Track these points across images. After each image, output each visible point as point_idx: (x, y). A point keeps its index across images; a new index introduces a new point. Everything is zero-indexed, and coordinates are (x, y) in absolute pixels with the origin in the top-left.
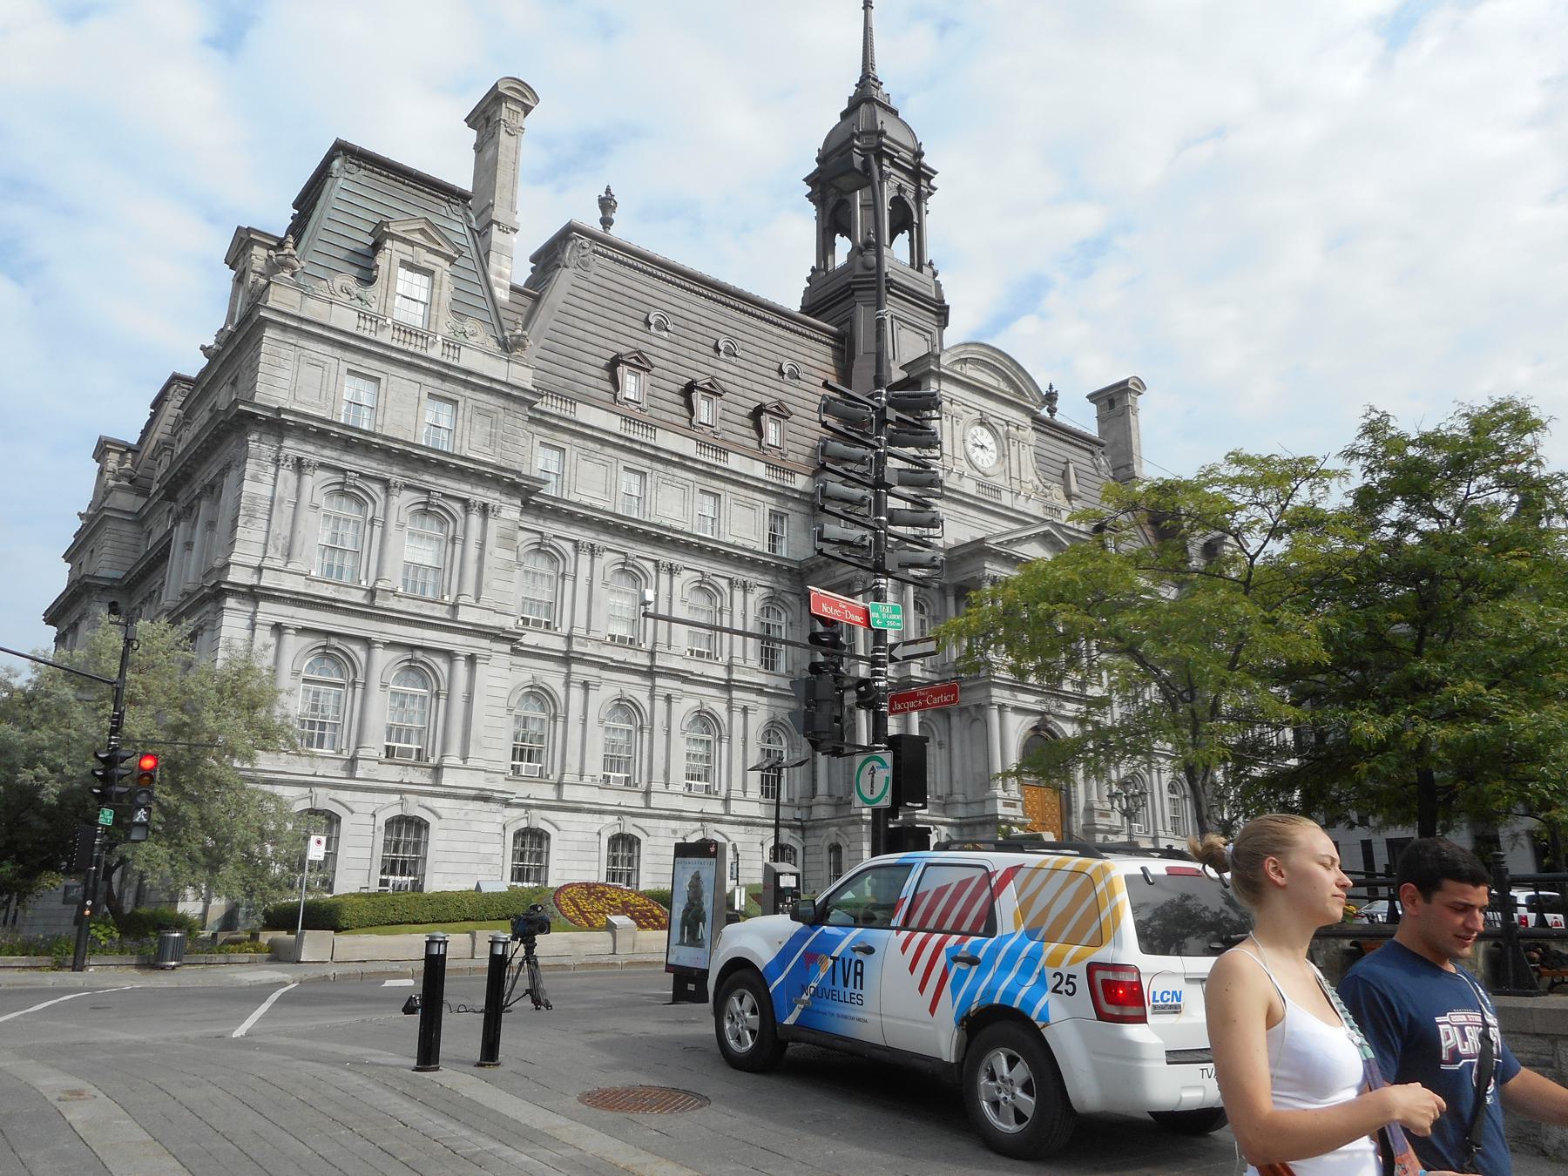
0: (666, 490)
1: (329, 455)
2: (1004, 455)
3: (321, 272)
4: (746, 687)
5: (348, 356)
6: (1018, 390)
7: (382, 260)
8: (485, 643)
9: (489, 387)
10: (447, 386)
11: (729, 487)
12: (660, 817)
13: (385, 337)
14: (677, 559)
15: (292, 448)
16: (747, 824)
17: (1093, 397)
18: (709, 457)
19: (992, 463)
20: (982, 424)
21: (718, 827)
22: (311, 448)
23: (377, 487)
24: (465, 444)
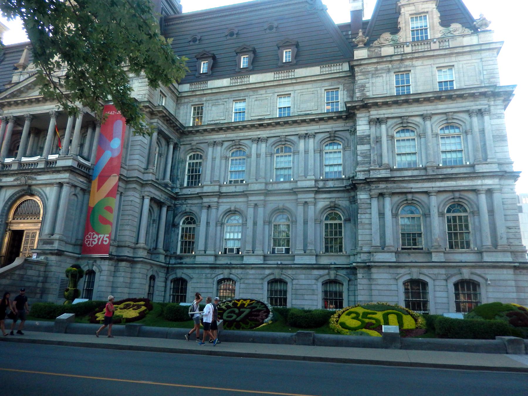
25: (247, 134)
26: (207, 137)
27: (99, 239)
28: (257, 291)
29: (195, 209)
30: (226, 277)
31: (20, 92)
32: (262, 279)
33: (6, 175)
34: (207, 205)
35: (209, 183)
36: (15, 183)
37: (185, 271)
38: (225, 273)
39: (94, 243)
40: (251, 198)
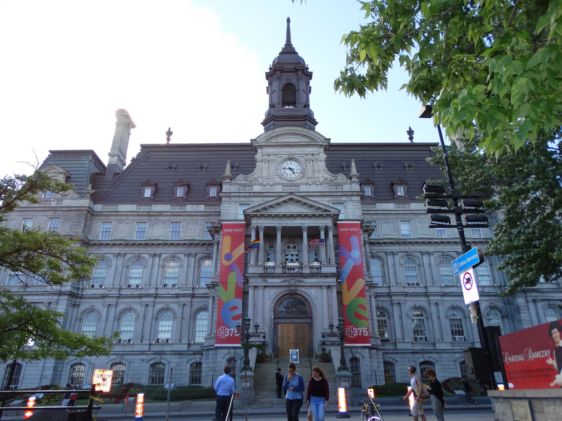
0: (155, 226)
4: (185, 296)
8: (56, 297)
11: (186, 218)
12: (136, 354)
14: (158, 250)
16: (179, 354)
18: (177, 209)
20: (290, 159)
21: (164, 356)
25: (416, 248)
26: (384, 248)
27: (358, 332)
28: (452, 370)
29: (386, 305)
30: (426, 360)
31: (271, 206)
32: (455, 361)
33: (273, 277)
34: (396, 302)
35: (395, 285)
36: (283, 284)
37: (390, 355)
38: (426, 357)
39: (355, 335)
40: (431, 298)
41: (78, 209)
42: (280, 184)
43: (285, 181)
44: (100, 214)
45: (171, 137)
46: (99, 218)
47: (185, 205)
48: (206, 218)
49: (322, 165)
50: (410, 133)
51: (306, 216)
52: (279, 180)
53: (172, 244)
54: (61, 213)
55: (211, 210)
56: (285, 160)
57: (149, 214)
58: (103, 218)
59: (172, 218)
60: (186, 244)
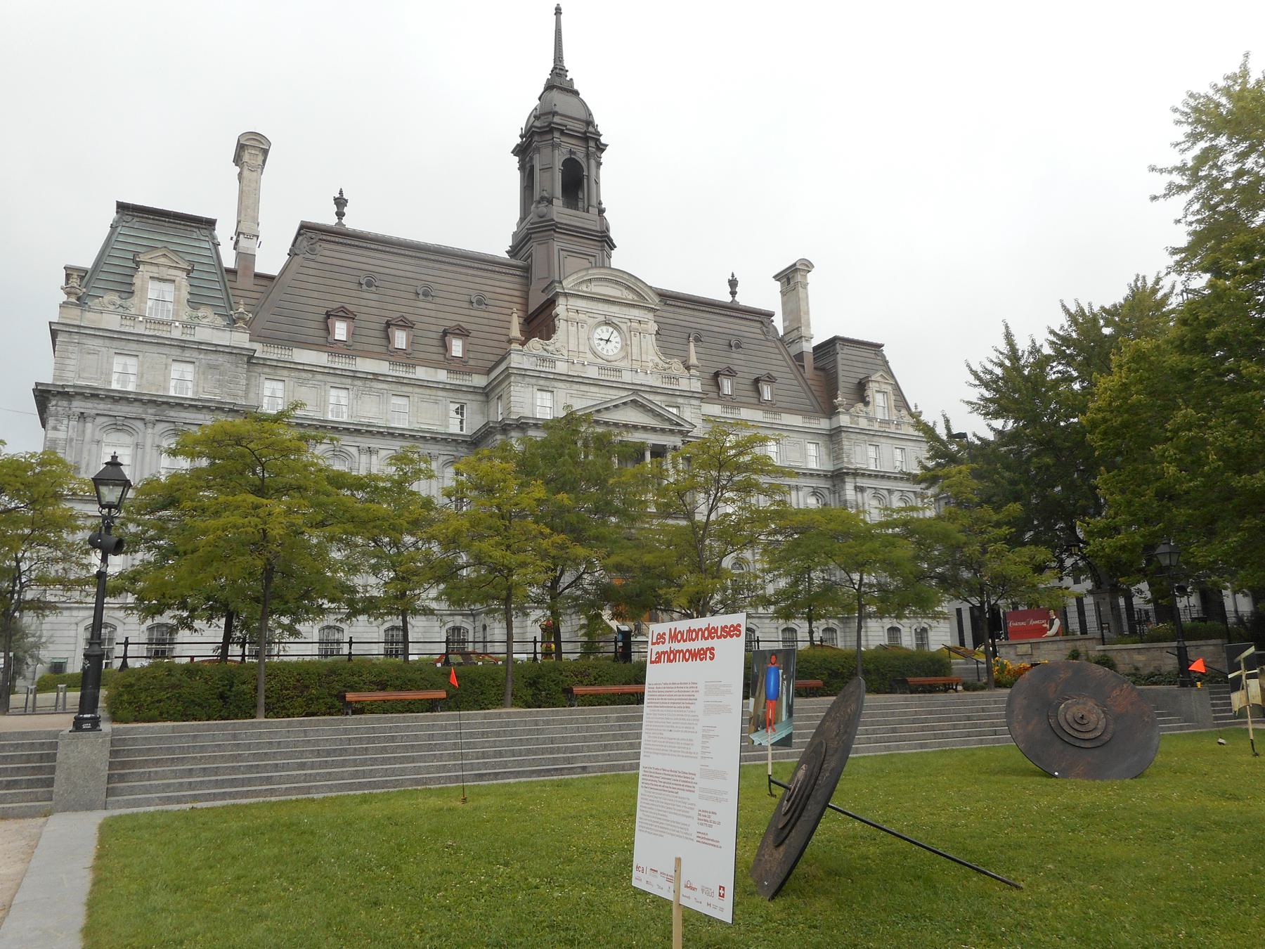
1: (102, 407)
2: (625, 346)
3: (99, 293)
5: (115, 343)
6: (639, 295)
7: (137, 280)
9: (216, 349)
10: (187, 353)
11: (417, 390)
13: (140, 329)
14: (374, 443)
15: (78, 406)
17: (778, 277)
18: (400, 372)
19: (616, 351)
22: (90, 405)
23: (139, 424)
24: (201, 390)
41: (233, 352)
42: (594, 364)
43: (600, 361)
44: (264, 363)
45: (345, 210)
46: (259, 369)
47: (414, 366)
48: (451, 394)
49: (650, 342)
50: (733, 283)
51: (654, 430)
52: (590, 356)
53: (402, 435)
54: (195, 354)
55: (458, 382)
56: (599, 324)
57: (354, 376)
58: (267, 370)
59: (394, 386)
60: (424, 438)
